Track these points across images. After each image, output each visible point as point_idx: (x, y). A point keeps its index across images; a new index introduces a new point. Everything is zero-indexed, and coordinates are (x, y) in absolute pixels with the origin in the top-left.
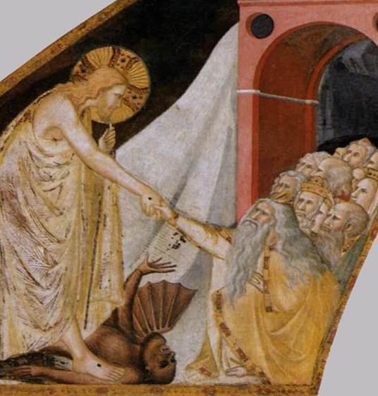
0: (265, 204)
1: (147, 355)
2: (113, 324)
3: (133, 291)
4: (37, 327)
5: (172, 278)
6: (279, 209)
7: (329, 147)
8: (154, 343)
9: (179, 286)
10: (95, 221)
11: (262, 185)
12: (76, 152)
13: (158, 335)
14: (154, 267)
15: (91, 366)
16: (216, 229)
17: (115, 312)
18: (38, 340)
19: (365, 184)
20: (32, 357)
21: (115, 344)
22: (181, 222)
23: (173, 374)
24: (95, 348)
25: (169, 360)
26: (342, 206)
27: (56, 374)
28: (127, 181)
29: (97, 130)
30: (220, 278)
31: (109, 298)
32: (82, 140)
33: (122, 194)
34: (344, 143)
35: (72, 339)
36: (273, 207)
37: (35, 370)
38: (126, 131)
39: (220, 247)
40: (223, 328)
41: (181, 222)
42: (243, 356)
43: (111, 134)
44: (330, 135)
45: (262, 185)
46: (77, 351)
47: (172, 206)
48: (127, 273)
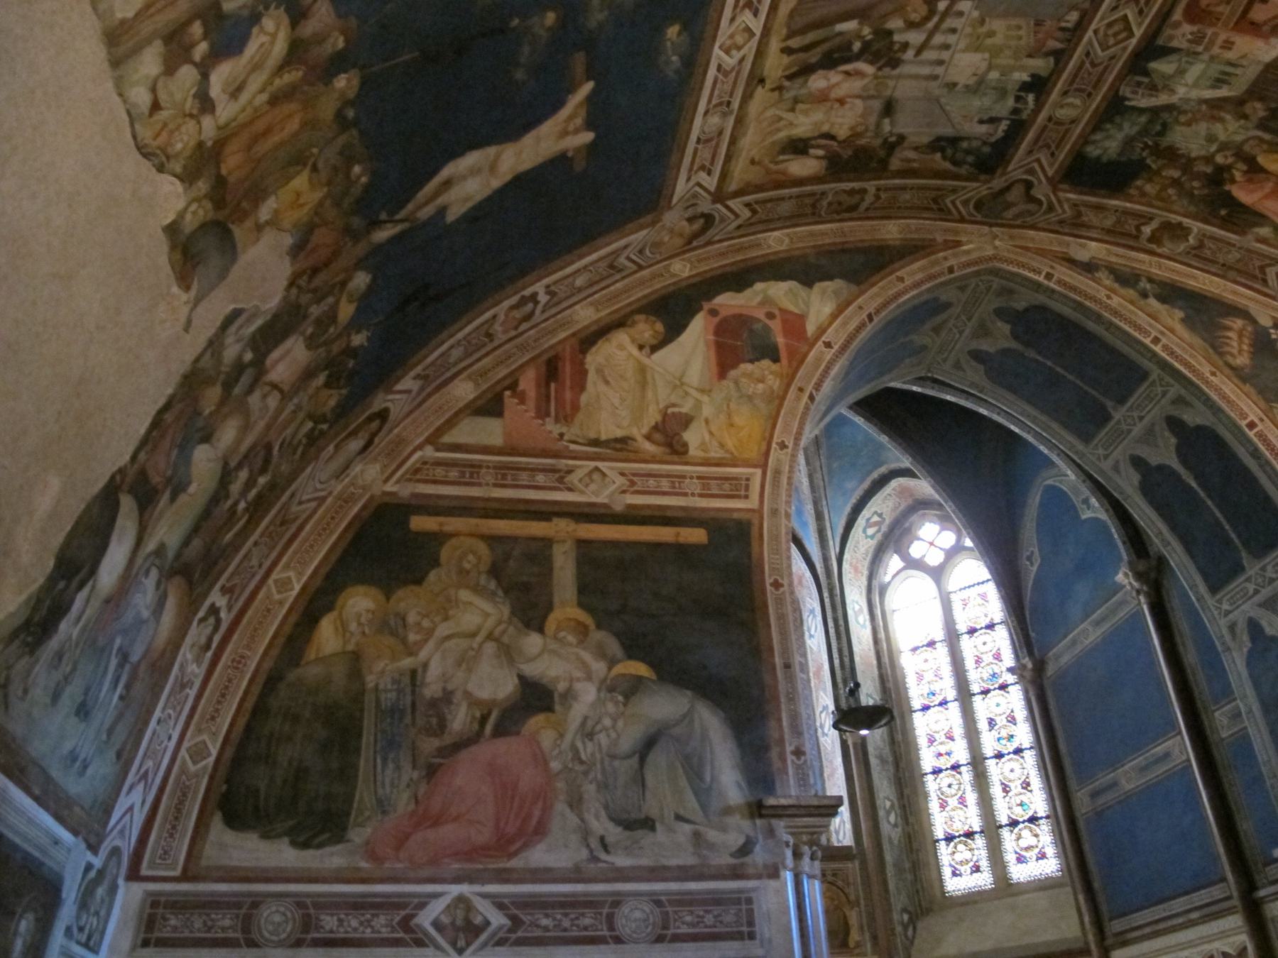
0: (725, 382)
1: (674, 442)
2: (656, 428)
3: (665, 415)
4: (618, 427)
5: (684, 410)
6: (732, 385)
7: (752, 361)
8: (677, 438)
9: (686, 414)
10: (643, 384)
11: (722, 374)
12: (631, 355)
13: (678, 434)
14: (674, 405)
15: (648, 447)
16: (702, 391)
17: (657, 423)
18: (619, 433)
19: (771, 377)
20: (617, 440)
21: (657, 436)
22: (685, 388)
23: (686, 452)
24: (648, 437)
25: (685, 445)
26: (760, 386)
27: (629, 448)
28: (658, 369)
29: (641, 347)
30: (707, 411)
31: (653, 417)
32: (635, 352)
33: (657, 376)
34: (758, 360)
35: (638, 433)
36: (728, 384)
37: (618, 446)
38: (654, 349)
39: (705, 399)
40: (711, 433)
41: (685, 388)
42: (722, 446)
43: (647, 350)
44: (752, 357)
45: (722, 374)
46: (639, 438)
47: (680, 380)
48: (661, 406)
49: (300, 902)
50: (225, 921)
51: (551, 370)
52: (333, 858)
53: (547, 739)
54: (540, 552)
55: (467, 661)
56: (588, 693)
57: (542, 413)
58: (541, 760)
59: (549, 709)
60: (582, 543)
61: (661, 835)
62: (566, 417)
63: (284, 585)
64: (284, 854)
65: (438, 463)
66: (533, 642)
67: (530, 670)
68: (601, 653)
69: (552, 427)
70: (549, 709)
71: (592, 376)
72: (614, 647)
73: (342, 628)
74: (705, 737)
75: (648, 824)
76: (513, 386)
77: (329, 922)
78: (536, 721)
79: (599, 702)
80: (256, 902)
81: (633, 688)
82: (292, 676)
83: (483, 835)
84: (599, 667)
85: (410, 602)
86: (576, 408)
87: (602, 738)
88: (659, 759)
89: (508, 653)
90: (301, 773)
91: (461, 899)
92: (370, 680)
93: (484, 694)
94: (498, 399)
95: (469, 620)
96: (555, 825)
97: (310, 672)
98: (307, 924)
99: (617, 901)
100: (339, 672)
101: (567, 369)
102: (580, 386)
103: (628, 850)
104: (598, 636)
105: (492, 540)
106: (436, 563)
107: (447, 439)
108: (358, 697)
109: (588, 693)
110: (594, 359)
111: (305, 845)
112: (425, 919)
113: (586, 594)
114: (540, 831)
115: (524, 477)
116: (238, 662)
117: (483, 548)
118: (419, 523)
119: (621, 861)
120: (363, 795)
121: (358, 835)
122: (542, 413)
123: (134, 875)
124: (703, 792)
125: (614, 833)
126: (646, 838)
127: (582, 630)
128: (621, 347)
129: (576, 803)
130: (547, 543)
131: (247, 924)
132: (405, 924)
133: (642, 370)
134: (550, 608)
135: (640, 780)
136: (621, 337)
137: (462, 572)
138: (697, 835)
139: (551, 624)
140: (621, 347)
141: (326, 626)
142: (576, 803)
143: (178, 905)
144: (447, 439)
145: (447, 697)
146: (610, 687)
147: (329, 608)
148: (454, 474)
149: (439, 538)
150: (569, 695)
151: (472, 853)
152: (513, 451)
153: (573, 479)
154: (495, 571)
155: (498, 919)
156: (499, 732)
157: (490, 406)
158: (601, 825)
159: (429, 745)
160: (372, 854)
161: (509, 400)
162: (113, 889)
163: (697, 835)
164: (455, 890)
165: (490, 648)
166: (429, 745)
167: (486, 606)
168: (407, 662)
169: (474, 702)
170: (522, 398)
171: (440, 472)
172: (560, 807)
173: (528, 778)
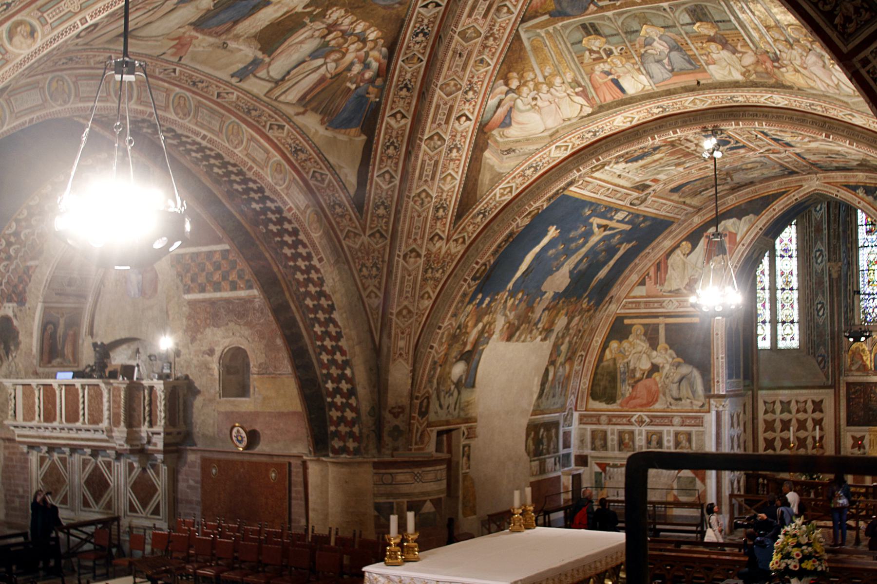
18: (677, 288)
32: (682, 256)
38: (688, 254)
49: (608, 416)
50: (594, 419)
51: (658, 267)
52: (614, 406)
53: (658, 379)
54: (656, 328)
55: (639, 359)
56: (667, 367)
57: (656, 283)
58: (656, 384)
59: (658, 371)
60: (666, 324)
61: (683, 401)
62: (662, 284)
63: (597, 342)
64: (603, 406)
65: (630, 303)
66: (654, 353)
67: (654, 361)
68: (671, 356)
69: (658, 287)
70: (658, 371)
71: (670, 268)
72: (675, 355)
73: (611, 352)
74: (695, 377)
75: (680, 399)
76: (648, 274)
77: (614, 420)
78: (655, 375)
79: (670, 369)
80: (600, 416)
81: (678, 365)
82: (602, 364)
83: (645, 402)
84: (670, 360)
85: (625, 344)
86: (665, 280)
87: (670, 378)
88: (684, 383)
89: (649, 356)
90: (606, 388)
91: (640, 416)
92: (618, 365)
93: (643, 368)
94: (644, 278)
95: (639, 349)
96: (659, 400)
97: (605, 364)
98: (610, 420)
99: (673, 417)
100: (611, 363)
101: (662, 265)
102: (666, 272)
103: (676, 405)
104: (670, 351)
105: (644, 325)
106: (631, 333)
107: (632, 294)
108: (616, 369)
109: (667, 367)
110: (670, 261)
111: (608, 404)
112: (633, 420)
113: (668, 340)
114: (657, 400)
115: (651, 305)
116: (590, 362)
117: (642, 328)
118: (626, 322)
119: (674, 408)
120: (619, 393)
121: (618, 402)
122: (656, 283)
123: (576, 410)
124: (694, 392)
125: (673, 401)
126: (680, 403)
127: (666, 350)
128: (678, 255)
129: (664, 394)
130: (658, 325)
131: (598, 420)
132: (629, 421)
133: (684, 263)
134: (658, 344)
135: (679, 389)
136: (678, 251)
137: (637, 335)
138: (691, 403)
139: (658, 348)
140: (678, 255)
141: (607, 352)
142: (664, 394)
143: (585, 416)
144: (632, 294)
145: (635, 368)
146: (672, 365)
147: (607, 347)
148: (634, 305)
149: (632, 325)
150: (663, 367)
151: (642, 406)
152: (649, 297)
153: (664, 304)
154: (645, 334)
155: (648, 420)
156: (647, 377)
157: (642, 283)
158: (670, 400)
159: (631, 381)
160: (621, 405)
161: (647, 280)
162: (572, 414)
163: (691, 403)
164: (639, 413)
165: (644, 356)
166: (631, 381)
167: (643, 344)
168: (626, 360)
169: (641, 370)
170: (650, 278)
171: (630, 305)
172: (661, 395)
173: (654, 388)
